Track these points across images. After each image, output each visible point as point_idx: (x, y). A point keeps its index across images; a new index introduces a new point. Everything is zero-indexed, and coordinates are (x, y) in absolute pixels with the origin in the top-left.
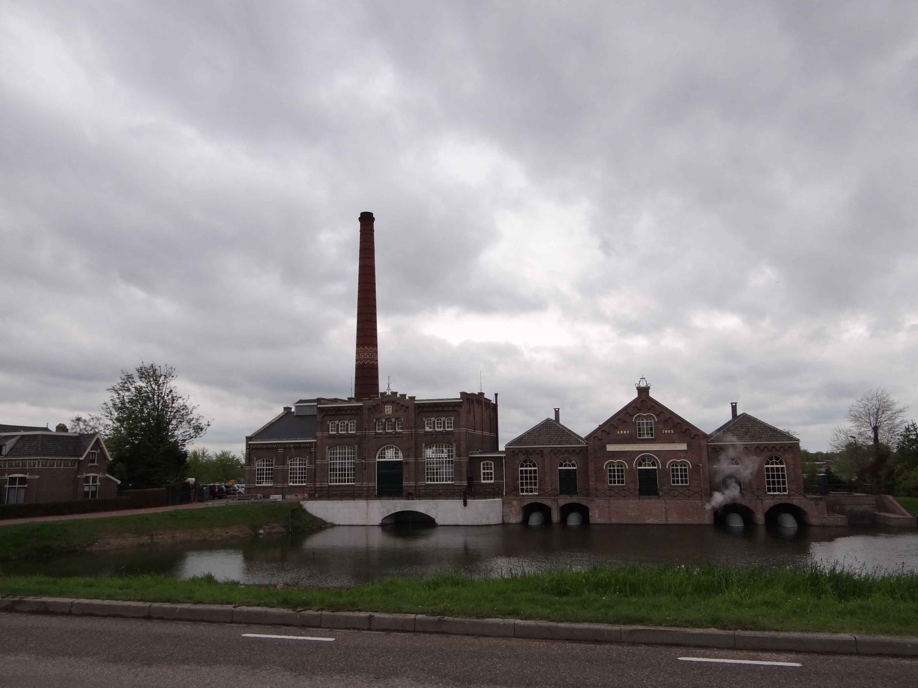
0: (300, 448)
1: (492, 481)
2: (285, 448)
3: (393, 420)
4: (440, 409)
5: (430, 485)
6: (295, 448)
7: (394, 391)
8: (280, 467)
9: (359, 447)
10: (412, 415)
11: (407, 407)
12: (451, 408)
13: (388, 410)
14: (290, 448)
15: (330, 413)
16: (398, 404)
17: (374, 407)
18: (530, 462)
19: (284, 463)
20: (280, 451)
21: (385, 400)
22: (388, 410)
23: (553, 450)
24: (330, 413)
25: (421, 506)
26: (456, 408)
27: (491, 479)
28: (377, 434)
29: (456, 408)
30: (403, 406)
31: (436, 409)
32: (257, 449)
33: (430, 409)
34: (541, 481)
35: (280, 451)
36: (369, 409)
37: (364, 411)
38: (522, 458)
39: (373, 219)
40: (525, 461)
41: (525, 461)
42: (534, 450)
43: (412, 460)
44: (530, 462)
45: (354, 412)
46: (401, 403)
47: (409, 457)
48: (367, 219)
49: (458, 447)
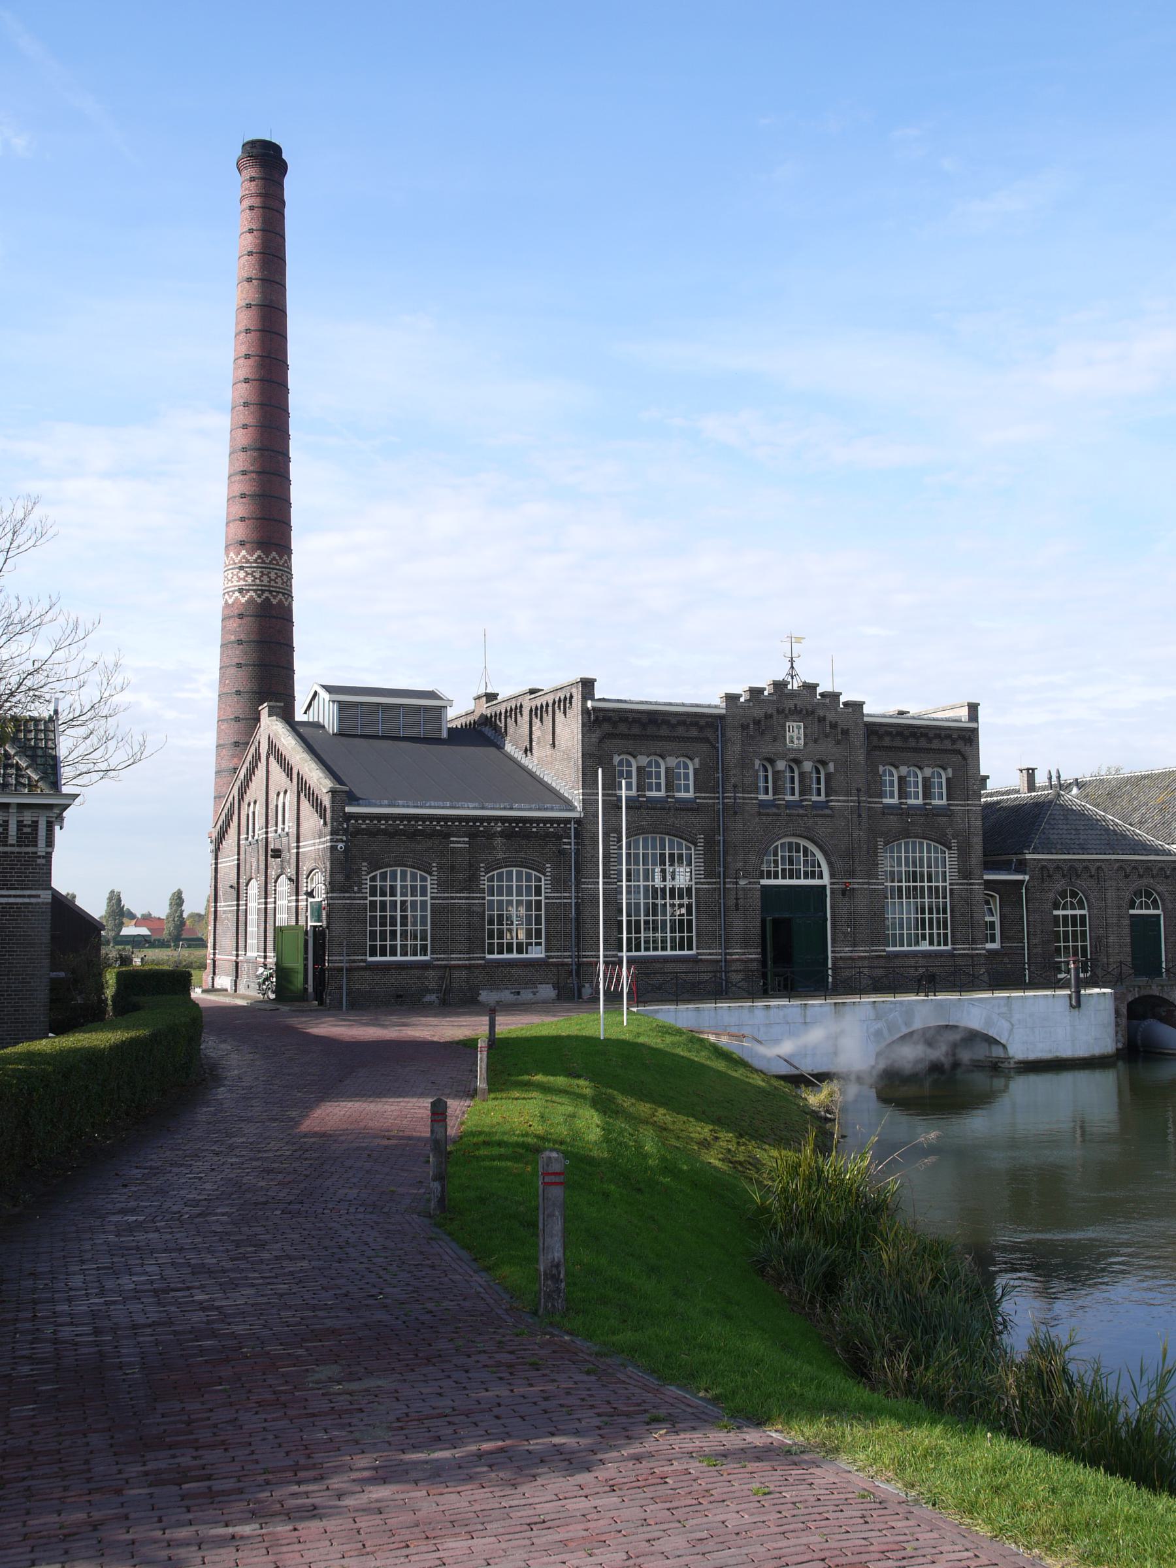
0: (528, 836)
1: (995, 946)
2: (473, 836)
3: (808, 766)
4: (923, 743)
5: (897, 955)
6: (508, 835)
7: (810, 680)
8: (459, 898)
9: (710, 844)
10: (860, 755)
11: (845, 732)
12: (947, 744)
13: (795, 734)
14: (490, 836)
15: (623, 728)
16: (822, 720)
17: (757, 722)
18: (1074, 895)
19: (471, 883)
20: (459, 842)
21: (789, 704)
22: (795, 734)
23: (1122, 866)
24: (623, 728)
25: (978, 1009)
26: (960, 745)
27: (993, 940)
28: (762, 804)
29: (960, 745)
30: (834, 726)
31: (912, 743)
32: (373, 833)
33: (898, 742)
34: (1098, 942)
35: (459, 842)
36: (744, 727)
37: (730, 733)
38: (1061, 884)
39: (282, 167)
40: (1063, 895)
41: (1063, 895)
42: (1086, 865)
43: (857, 883)
44: (1074, 895)
45: (694, 733)
46: (830, 717)
47: (851, 873)
48: (266, 160)
49: (964, 853)
